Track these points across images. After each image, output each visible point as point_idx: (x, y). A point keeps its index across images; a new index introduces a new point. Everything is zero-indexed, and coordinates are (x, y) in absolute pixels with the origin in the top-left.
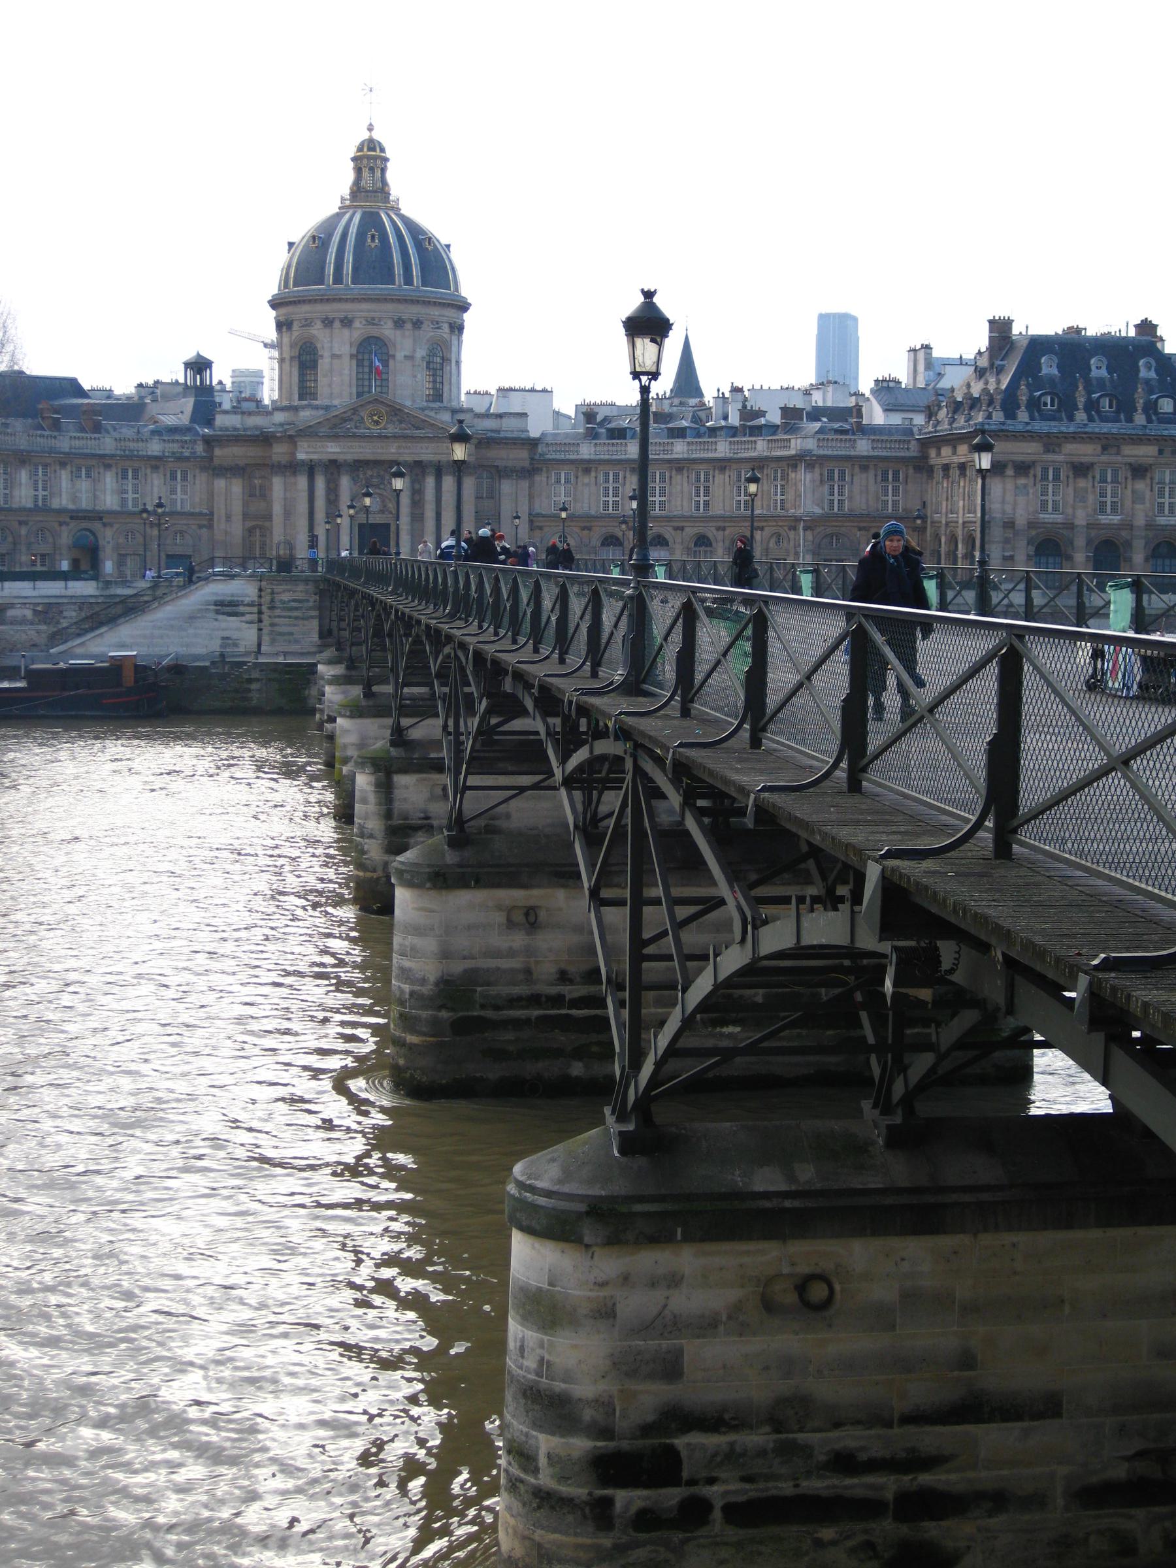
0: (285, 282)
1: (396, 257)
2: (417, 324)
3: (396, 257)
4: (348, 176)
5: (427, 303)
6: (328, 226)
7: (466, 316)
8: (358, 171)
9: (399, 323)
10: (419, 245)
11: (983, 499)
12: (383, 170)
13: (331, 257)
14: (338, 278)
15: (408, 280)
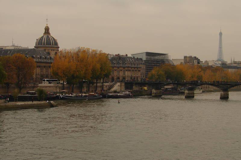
0: (36, 44)
1: (51, 42)
2: (54, 50)
3: (51, 42)
4: (44, 31)
5: (54, 47)
6: (42, 37)
7: (59, 49)
8: (46, 30)
9: (52, 50)
10: (54, 40)
11: (206, 100)
12: (49, 30)
13: (43, 42)
14: (44, 44)
15: (53, 45)
